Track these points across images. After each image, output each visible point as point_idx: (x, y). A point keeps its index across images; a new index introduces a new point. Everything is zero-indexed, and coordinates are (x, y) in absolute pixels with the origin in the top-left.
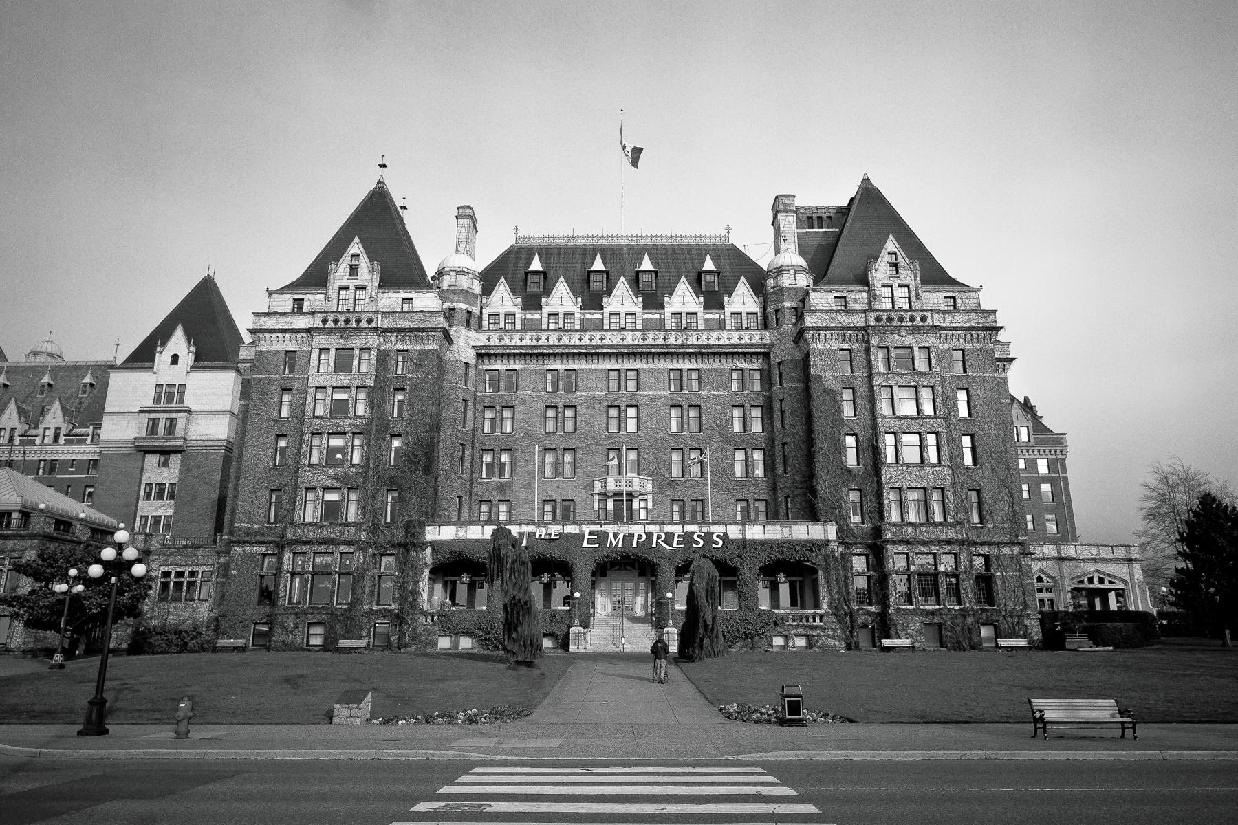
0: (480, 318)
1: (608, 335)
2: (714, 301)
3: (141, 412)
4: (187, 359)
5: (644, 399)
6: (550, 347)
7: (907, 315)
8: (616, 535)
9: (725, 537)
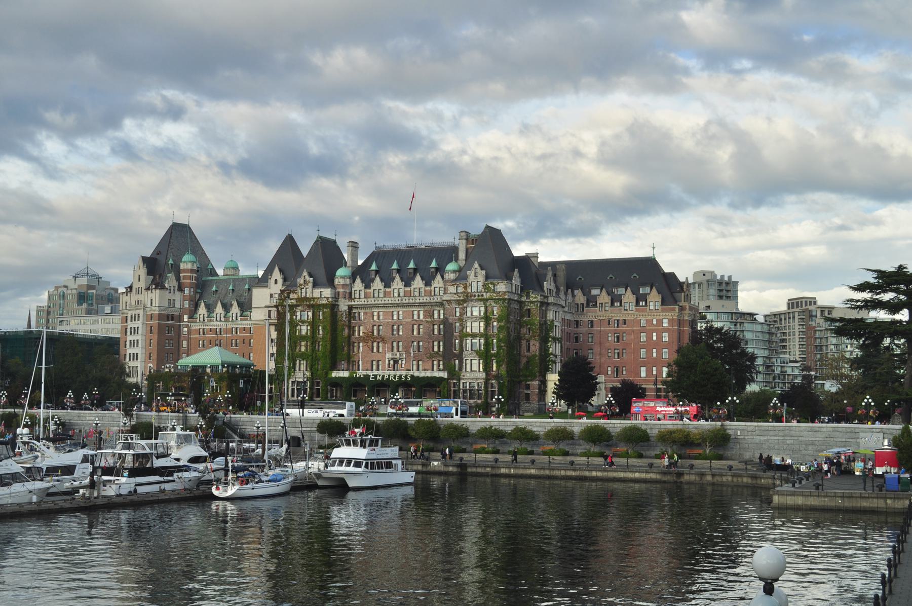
0: (350, 293)
1: (390, 299)
3: (265, 307)
4: (280, 281)
5: (404, 323)
6: (371, 304)
7: (477, 294)
8: (380, 376)
9: (412, 376)
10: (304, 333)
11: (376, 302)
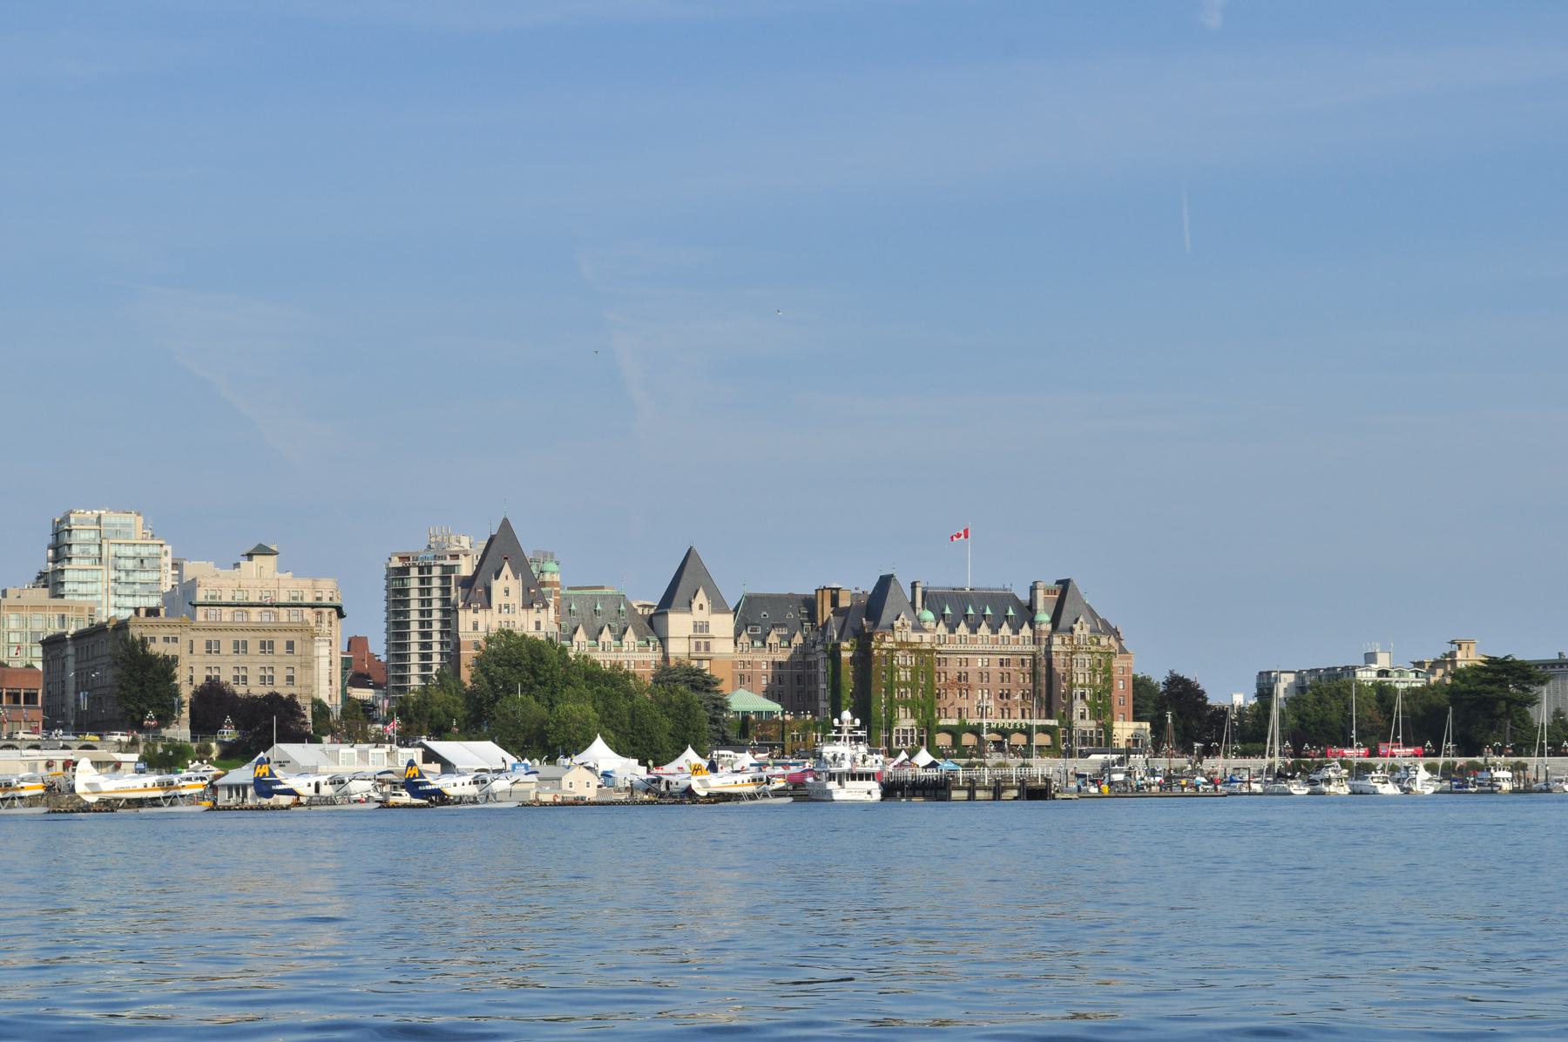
2: (1016, 632)
4: (706, 606)
9: (1026, 724)
10: (903, 679)
11: (966, 649)
